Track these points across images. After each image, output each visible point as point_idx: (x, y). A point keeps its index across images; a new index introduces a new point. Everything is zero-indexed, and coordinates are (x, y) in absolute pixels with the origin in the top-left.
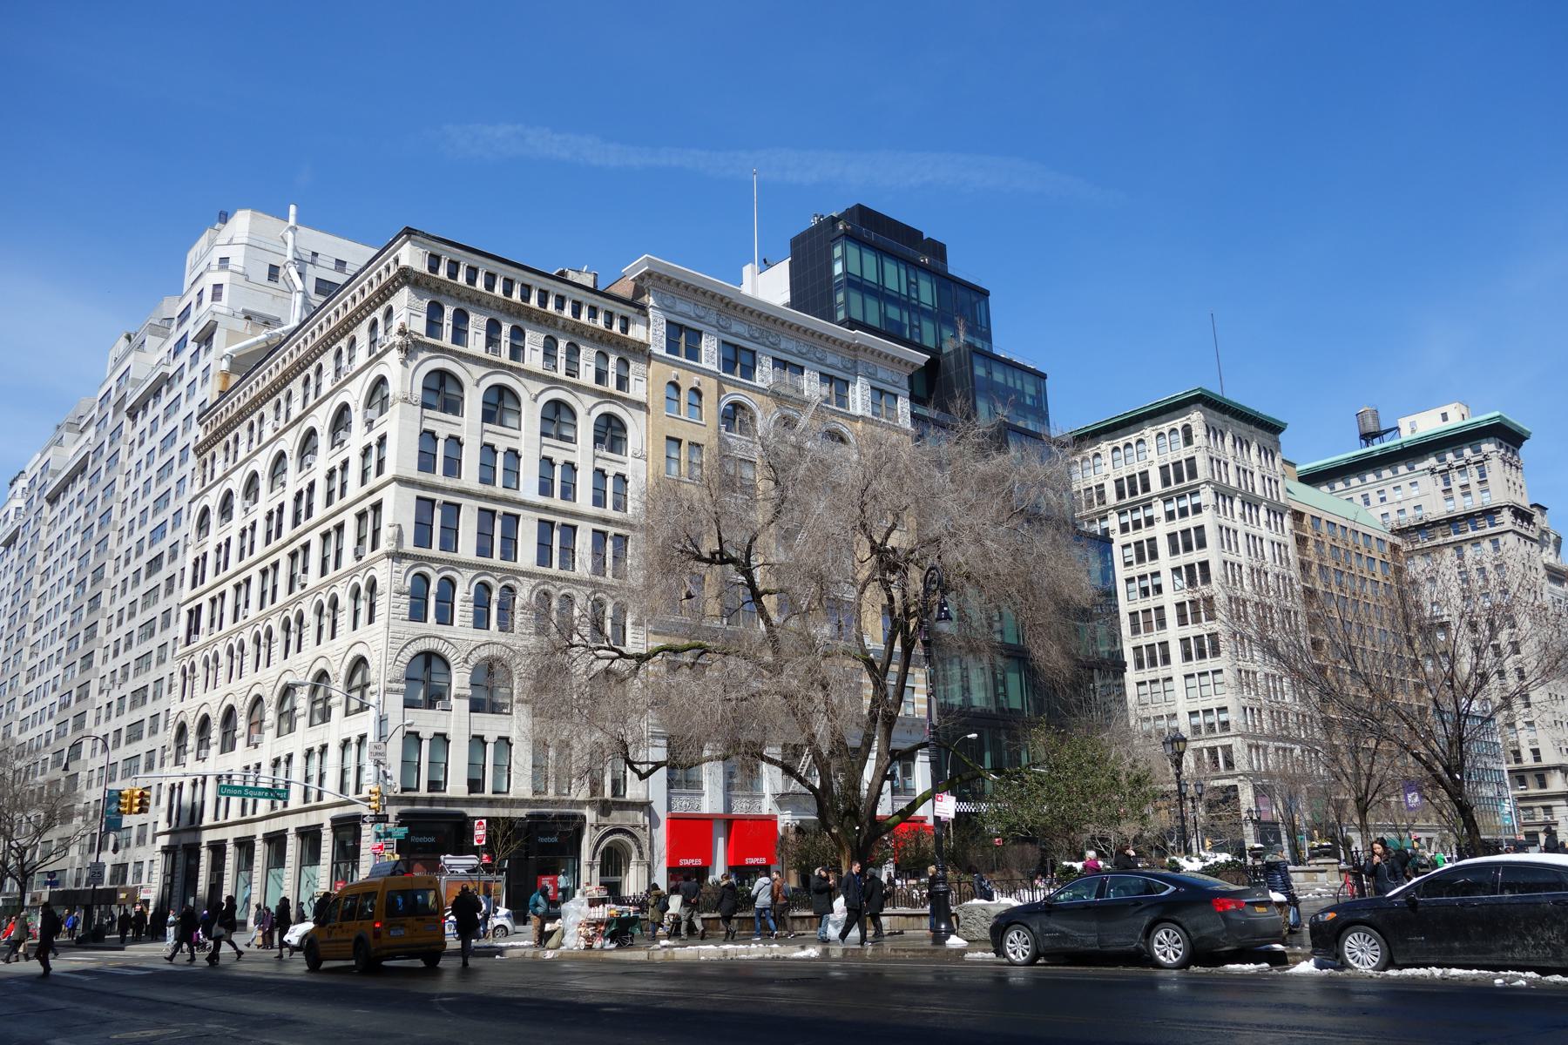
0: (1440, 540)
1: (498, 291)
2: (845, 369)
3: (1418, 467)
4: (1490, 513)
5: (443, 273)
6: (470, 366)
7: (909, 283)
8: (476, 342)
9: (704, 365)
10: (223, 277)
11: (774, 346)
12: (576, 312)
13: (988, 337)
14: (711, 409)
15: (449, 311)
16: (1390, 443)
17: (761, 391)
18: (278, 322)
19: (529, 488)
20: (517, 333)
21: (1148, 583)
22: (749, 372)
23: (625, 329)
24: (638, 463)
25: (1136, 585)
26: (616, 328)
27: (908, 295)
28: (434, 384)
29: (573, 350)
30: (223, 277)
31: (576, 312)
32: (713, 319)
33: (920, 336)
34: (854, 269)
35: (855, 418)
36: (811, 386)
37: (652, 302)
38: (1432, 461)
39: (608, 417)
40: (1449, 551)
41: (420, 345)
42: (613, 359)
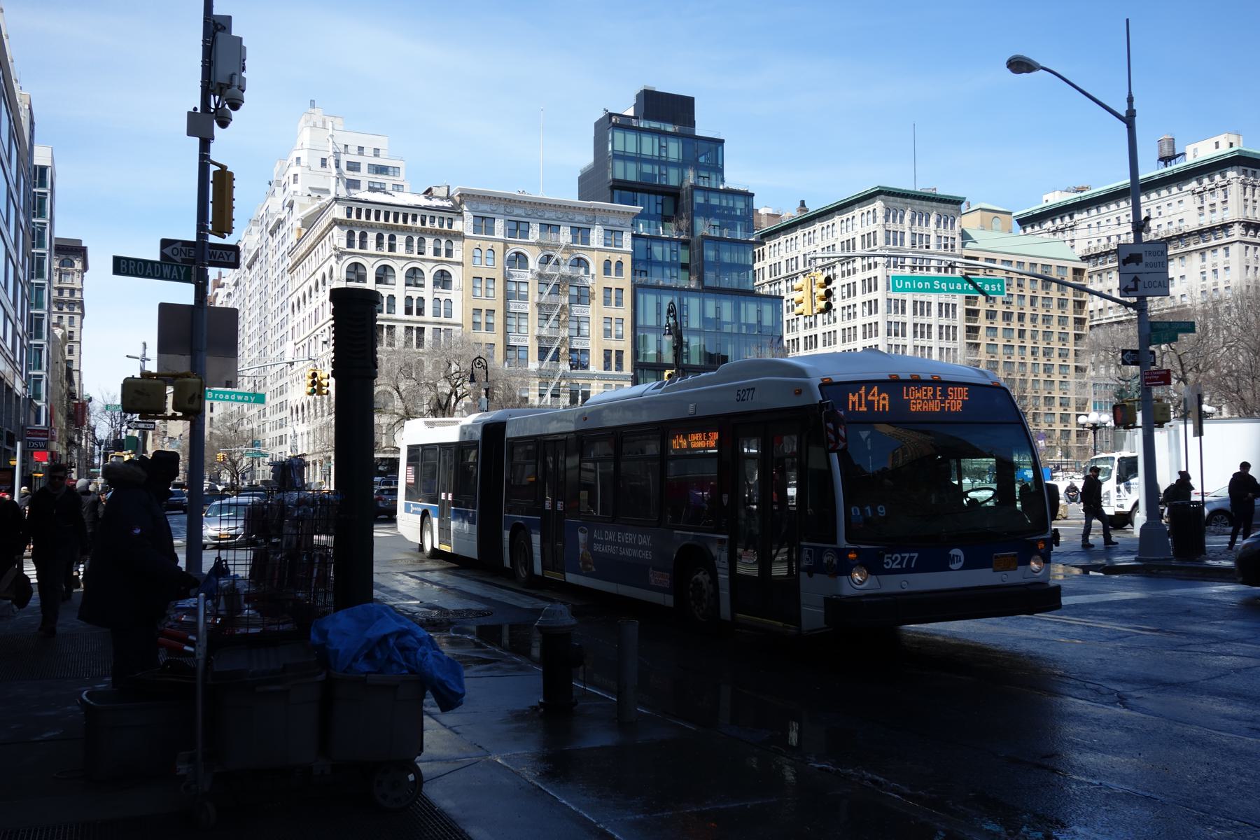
0: (1192, 247)
1: (382, 220)
2: (588, 222)
3: (1185, 188)
4: (1225, 227)
5: (354, 217)
6: (369, 259)
7: (660, 147)
8: (371, 246)
9: (496, 236)
10: (295, 169)
11: (541, 217)
12: (423, 223)
13: (718, 170)
15: (357, 233)
16: (1175, 167)
17: (532, 244)
18: (327, 191)
19: (400, 312)
20: (392, 238)
21: (851, 311)
22: (525, 234)
23: (450, 226)
24: (457, 295)
25: (846, 312)
26: (446, 227)
27: (660, 156)
28: (353, 269)
29: (421, 241)
30: (295, 169)
31: (423, 223)
32: (501, 210)
33: (666, 180)
34: (619, 147)
35: (593, 249)
36: (565, 236)
37: (465, 208)
38: (1194, 185)
39: (442, 271)
40: (1196, 256)
41: (343, 253)
42: (443, 241)
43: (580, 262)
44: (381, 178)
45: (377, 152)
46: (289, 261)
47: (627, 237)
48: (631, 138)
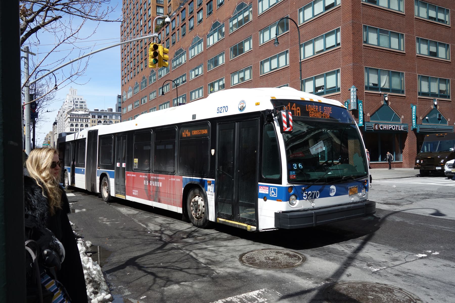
22: (101, 118)
34: (120, 101)
44: (82, 104)
45: (81, 99)
46: (65, 120)
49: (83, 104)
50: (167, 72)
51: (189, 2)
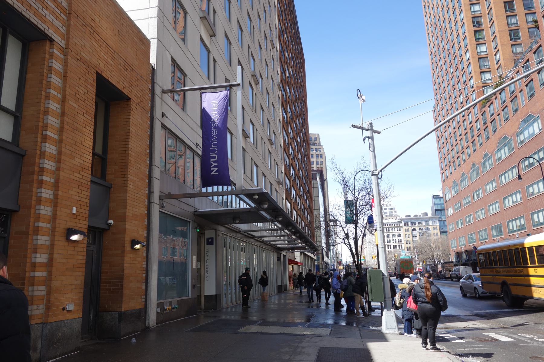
14: (410, 230)
22: (415, 225)
34: (436, 202)
43: (428, 228)
44: (392, 210)
45: (390, 205)
47: (438, 222)
48: (438, 200)
49: (393, 211)
50: (509, 152)
51: (534, 51)
